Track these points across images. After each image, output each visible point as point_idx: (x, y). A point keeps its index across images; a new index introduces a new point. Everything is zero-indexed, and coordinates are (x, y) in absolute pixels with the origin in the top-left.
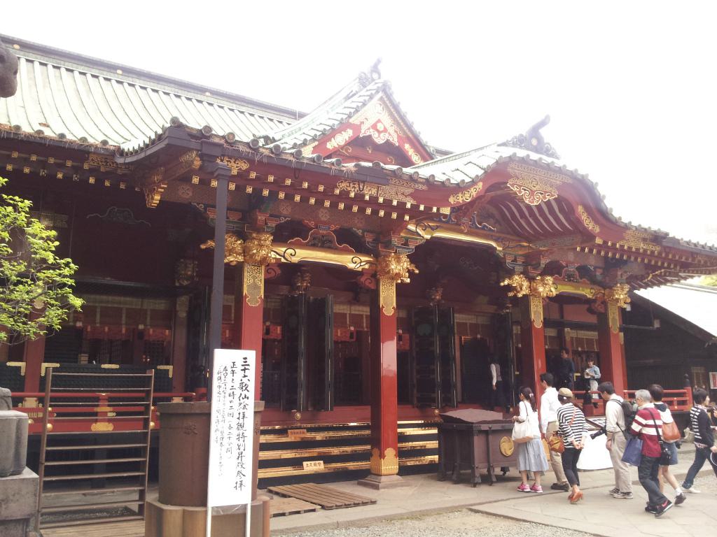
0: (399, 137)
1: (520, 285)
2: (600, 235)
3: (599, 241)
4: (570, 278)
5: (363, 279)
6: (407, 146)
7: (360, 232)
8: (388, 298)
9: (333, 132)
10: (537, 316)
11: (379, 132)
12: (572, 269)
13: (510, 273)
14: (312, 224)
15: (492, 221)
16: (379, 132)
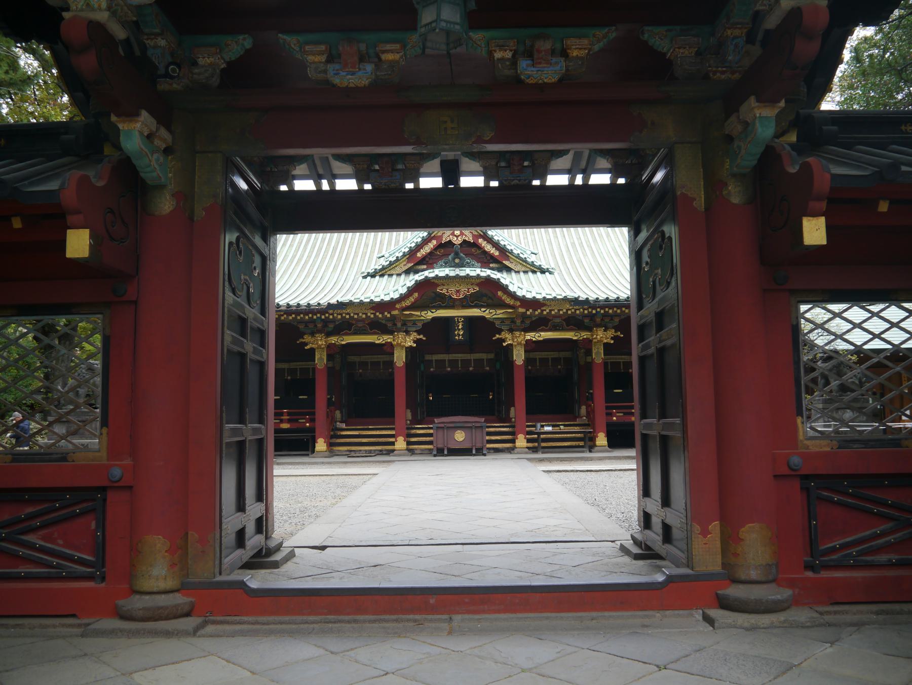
0: (474, 236)
1: (508, 339)
2: (520, 306)
3: (521, 310)
4: (555, 328)
5: (385, 347)
6: (480, 240)
7: (384, 322)
8: (400, 358)
9: (419, 247)
10: (519, 356)
11: (457, 237)
12: (558, 320)
13: (500, 331)
14: (354, 322)
15: (485, 298)
16: (457, 237)
